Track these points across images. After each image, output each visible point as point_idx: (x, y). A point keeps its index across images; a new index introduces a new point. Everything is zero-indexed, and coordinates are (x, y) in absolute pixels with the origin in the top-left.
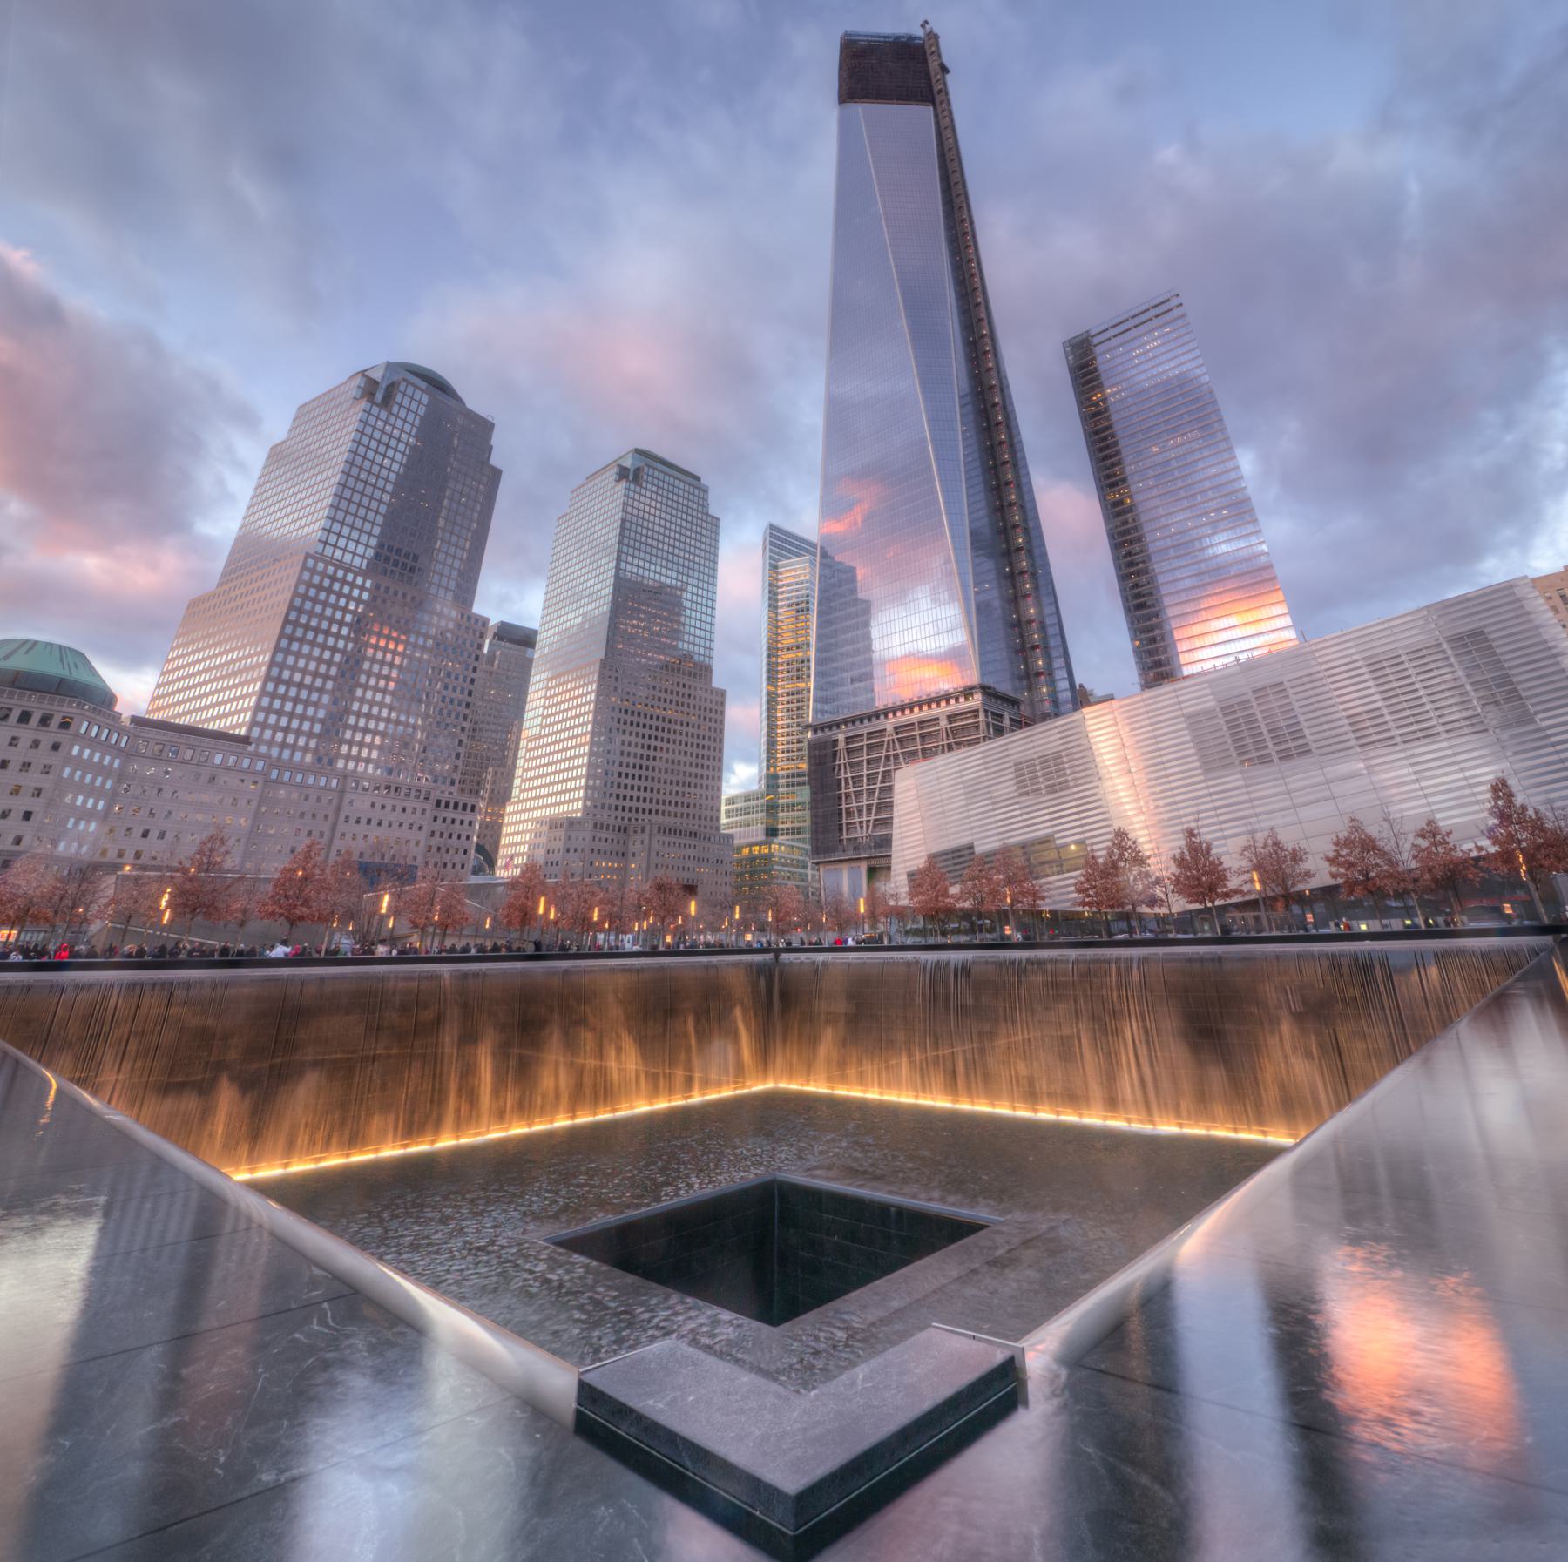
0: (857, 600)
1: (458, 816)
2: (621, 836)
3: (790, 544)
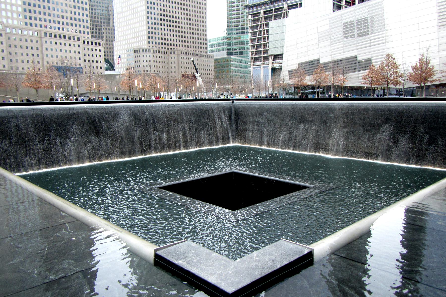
1: (94, 47)
2: (166, 56)
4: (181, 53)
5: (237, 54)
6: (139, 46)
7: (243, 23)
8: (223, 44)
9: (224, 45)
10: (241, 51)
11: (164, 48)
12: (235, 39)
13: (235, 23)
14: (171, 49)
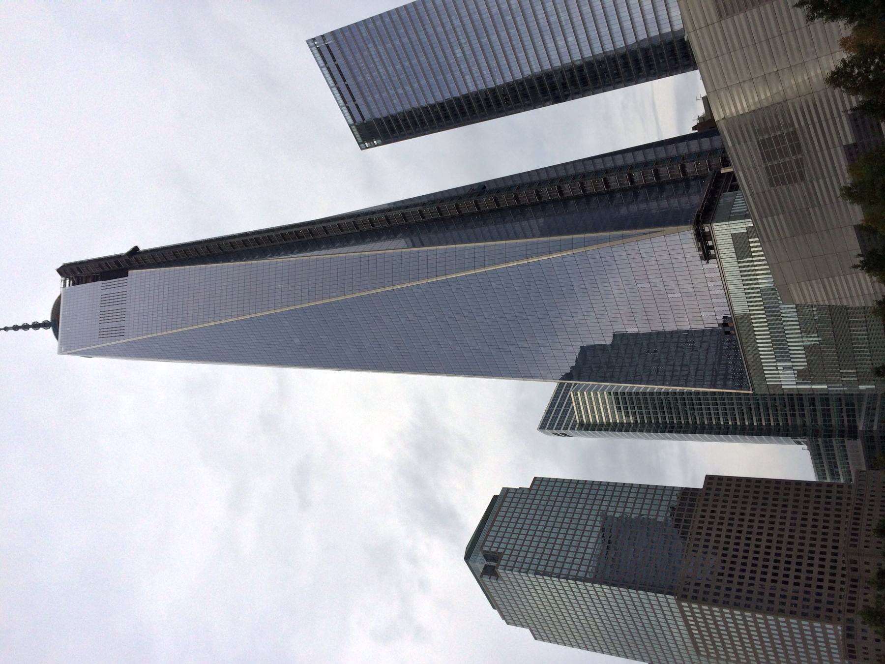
0: (612, 345)
3: (558, 410)
4: (855, 546)
5: (854, 416)
6: (837, 644)
7: (778, 401)
8: (829, 448)
9: (832, 446)
10: (844, 407)
11: (843, 586)
12: (816, 421)
13: (780, 419)
14: (843, 569)
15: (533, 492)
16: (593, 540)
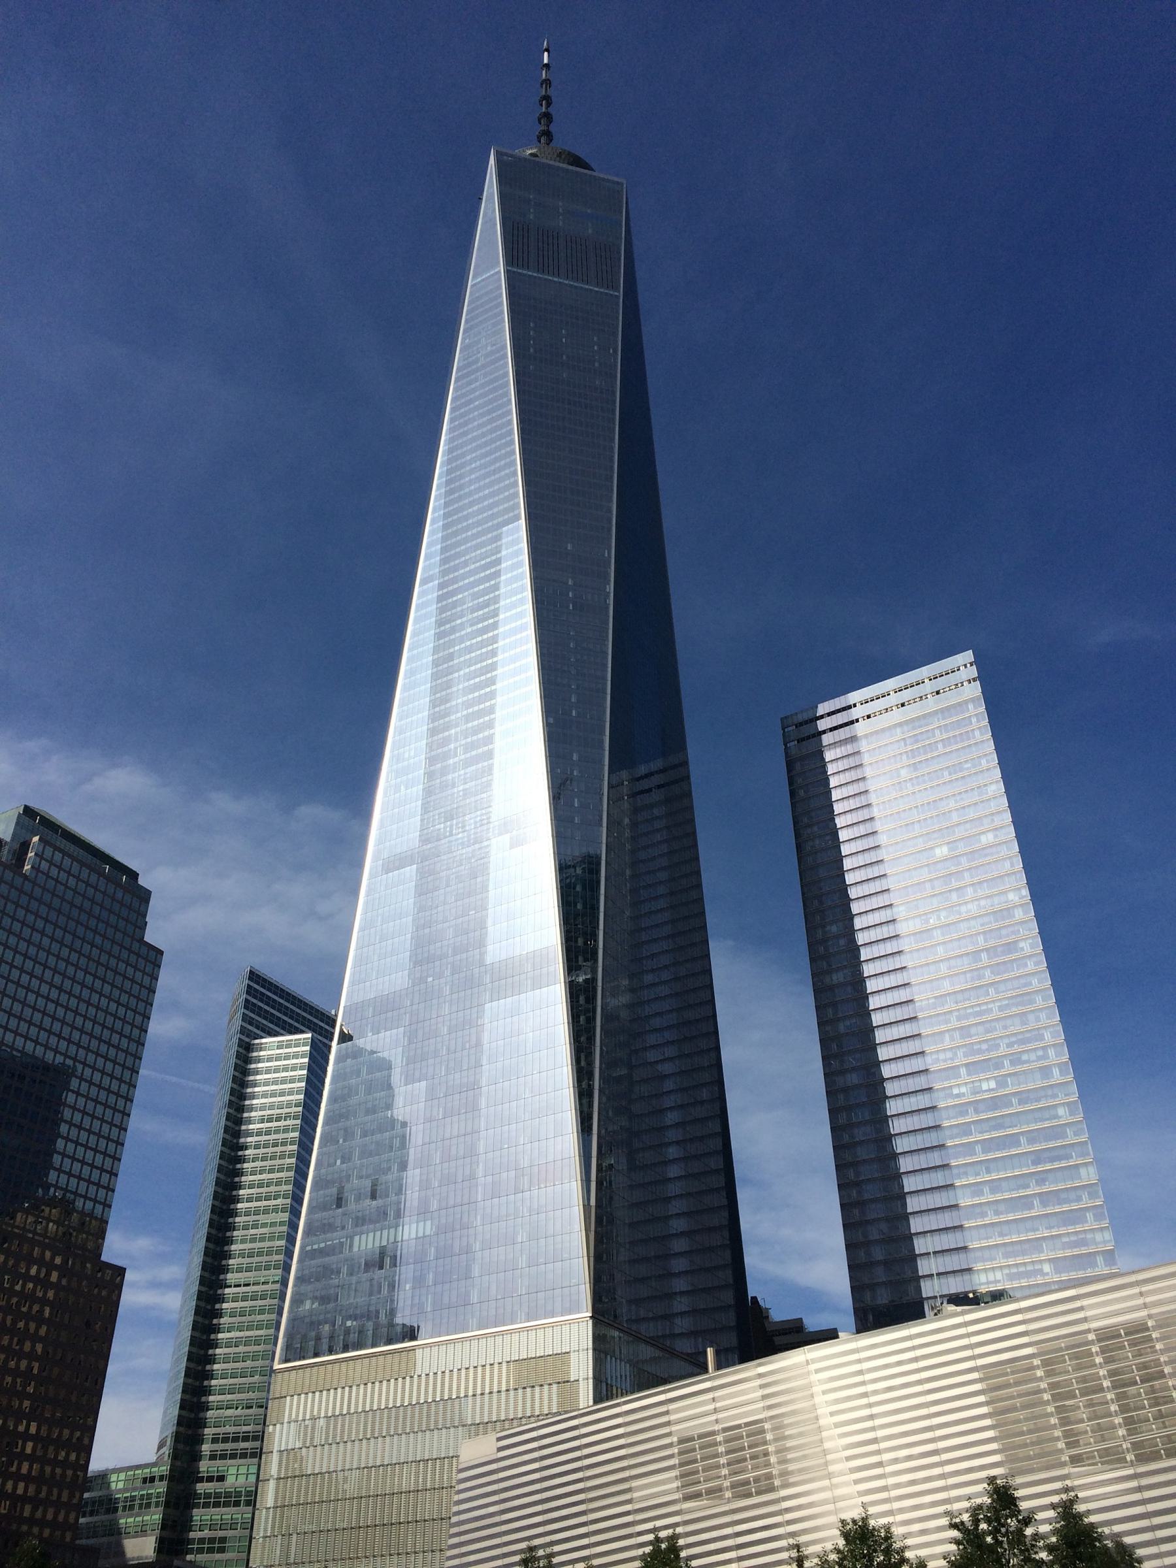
15: (136, 946)
16: (30, 1046)
